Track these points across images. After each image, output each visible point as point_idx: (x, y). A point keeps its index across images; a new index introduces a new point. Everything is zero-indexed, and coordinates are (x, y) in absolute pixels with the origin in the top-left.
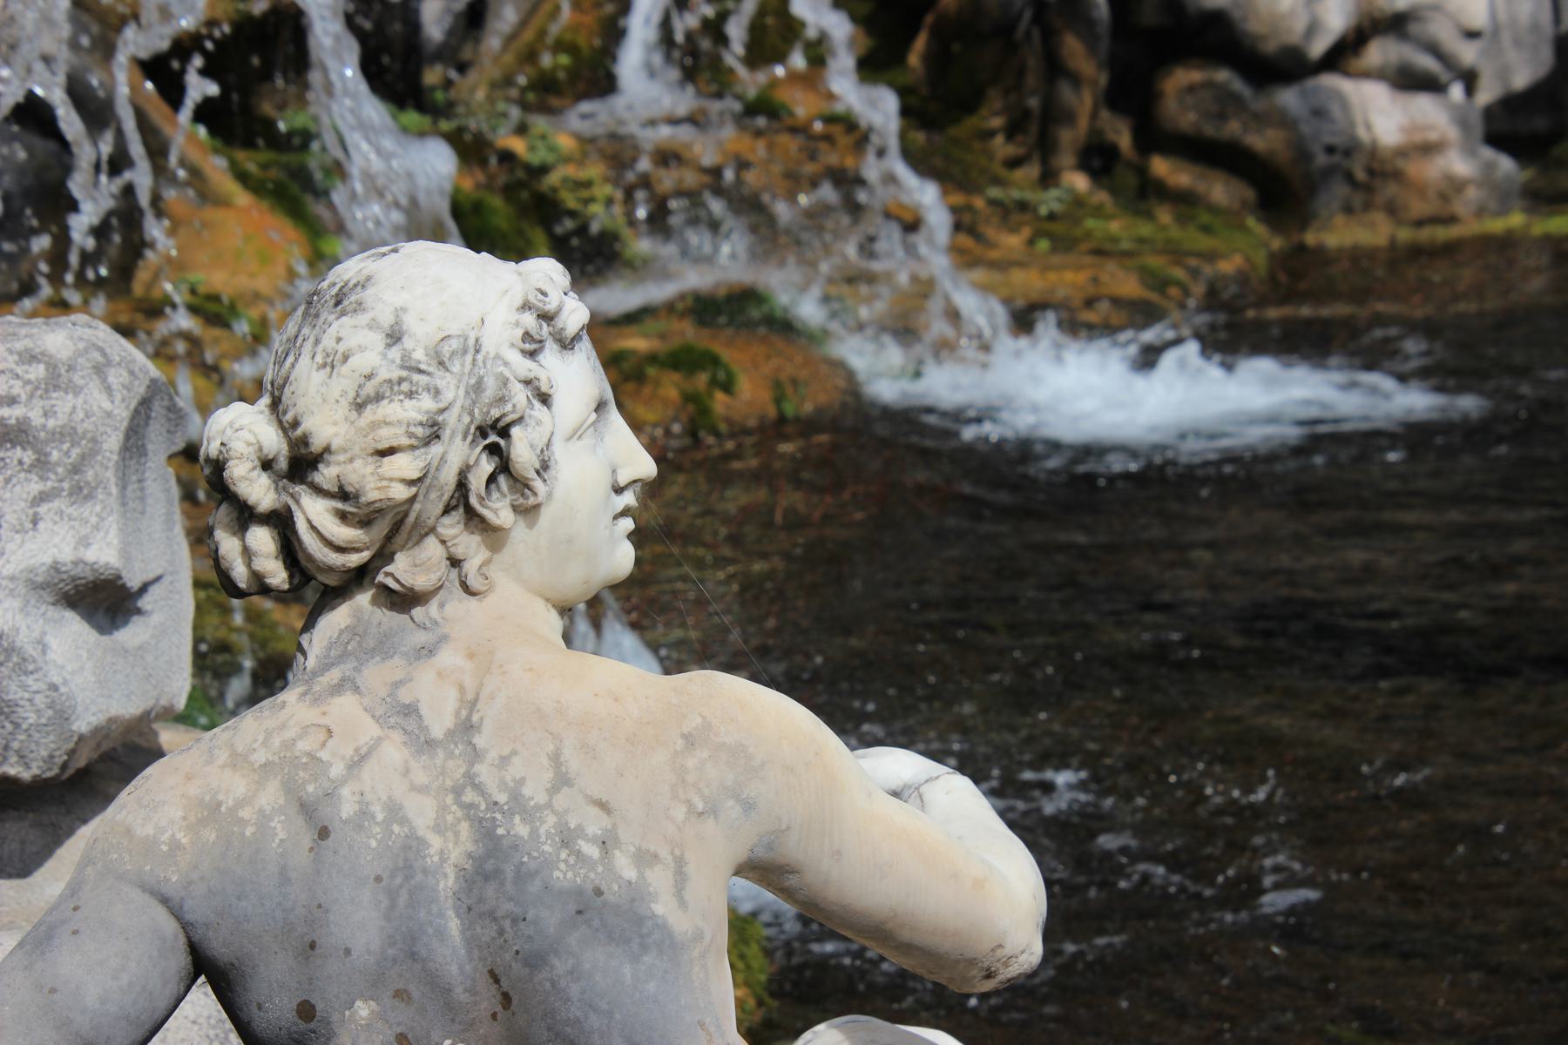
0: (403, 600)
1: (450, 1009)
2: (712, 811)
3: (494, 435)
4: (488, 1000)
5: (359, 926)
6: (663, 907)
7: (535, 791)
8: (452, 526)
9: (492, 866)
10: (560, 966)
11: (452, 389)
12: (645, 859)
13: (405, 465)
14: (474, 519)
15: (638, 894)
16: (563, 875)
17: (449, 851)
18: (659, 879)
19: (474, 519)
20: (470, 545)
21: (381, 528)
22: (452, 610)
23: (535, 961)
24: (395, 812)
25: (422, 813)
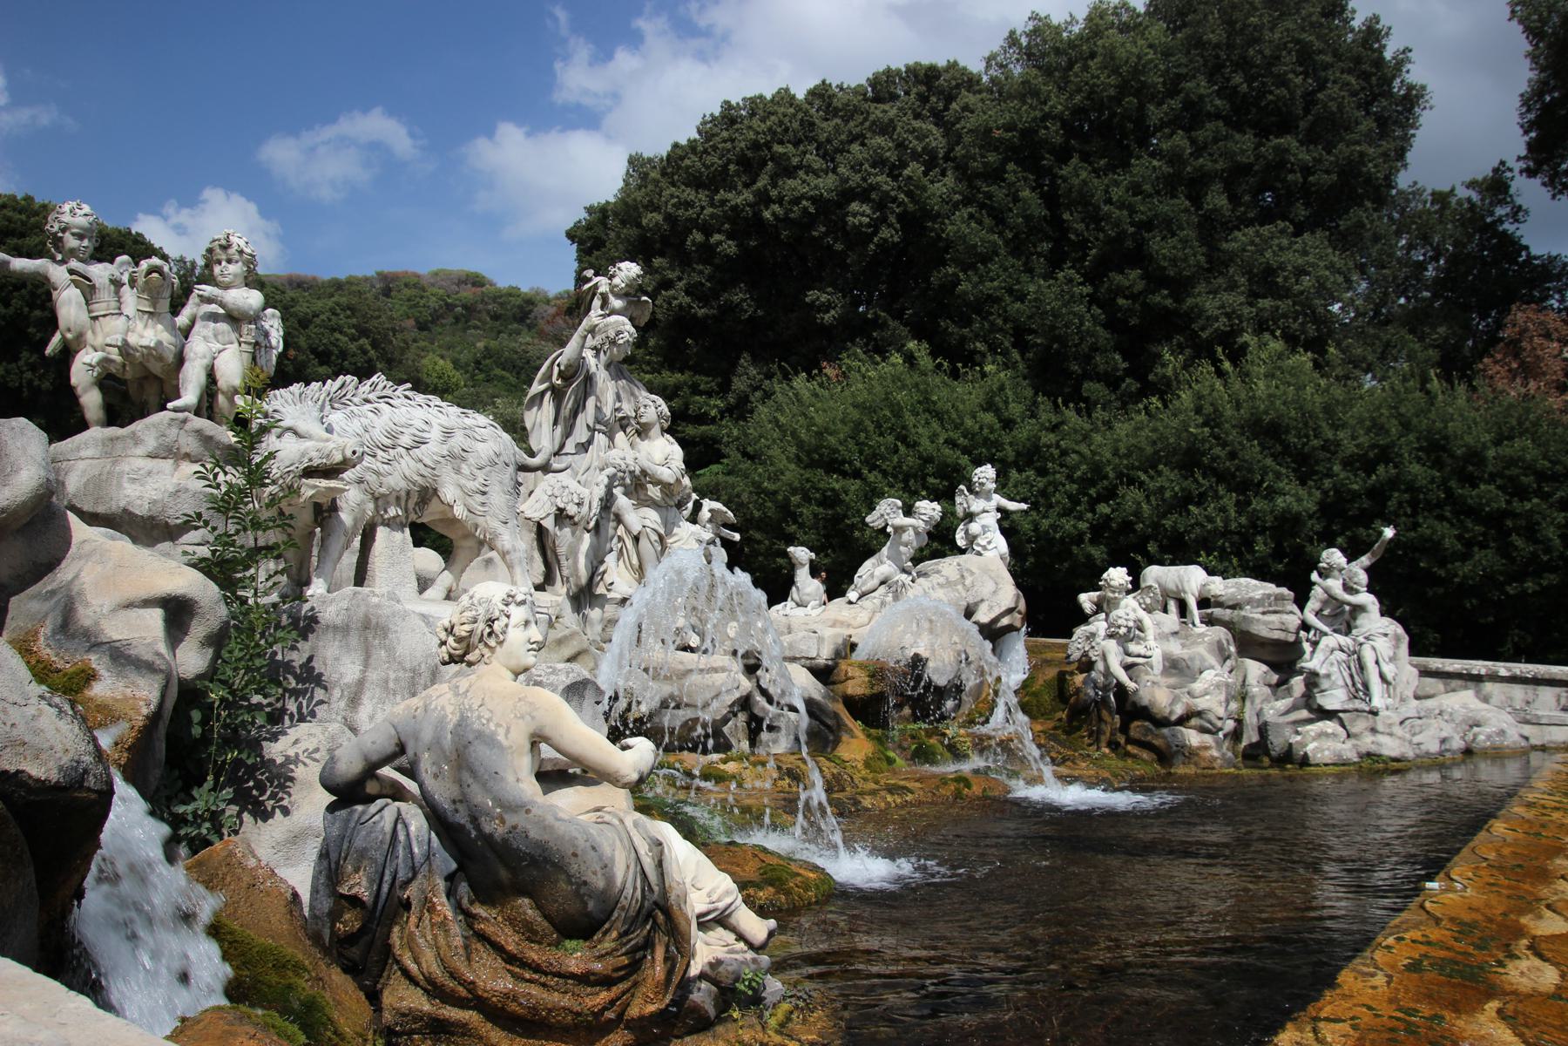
0: (470, 664)
1: (446, 757)
2: (522, 717)
3: (491, 622)
4: (454, 757)
5: (427, 735)
6: (501, 738)
7: (475, 707)
8: (481, 646)
9: (462, 723)
10: (472, 748)
11: (481, 610)
12: (498, 725)
13: (467, 627)
14: (486, 645)
15: (494, 733)
16: (476, 726)
17: (452, 719)
18: (501, 731)
19: (486, 645)
20: (486, 651)
21: (464, 645)
22: (480, 668)
23: (465, 747)
24: (443, 708)
25: (449, 709)
